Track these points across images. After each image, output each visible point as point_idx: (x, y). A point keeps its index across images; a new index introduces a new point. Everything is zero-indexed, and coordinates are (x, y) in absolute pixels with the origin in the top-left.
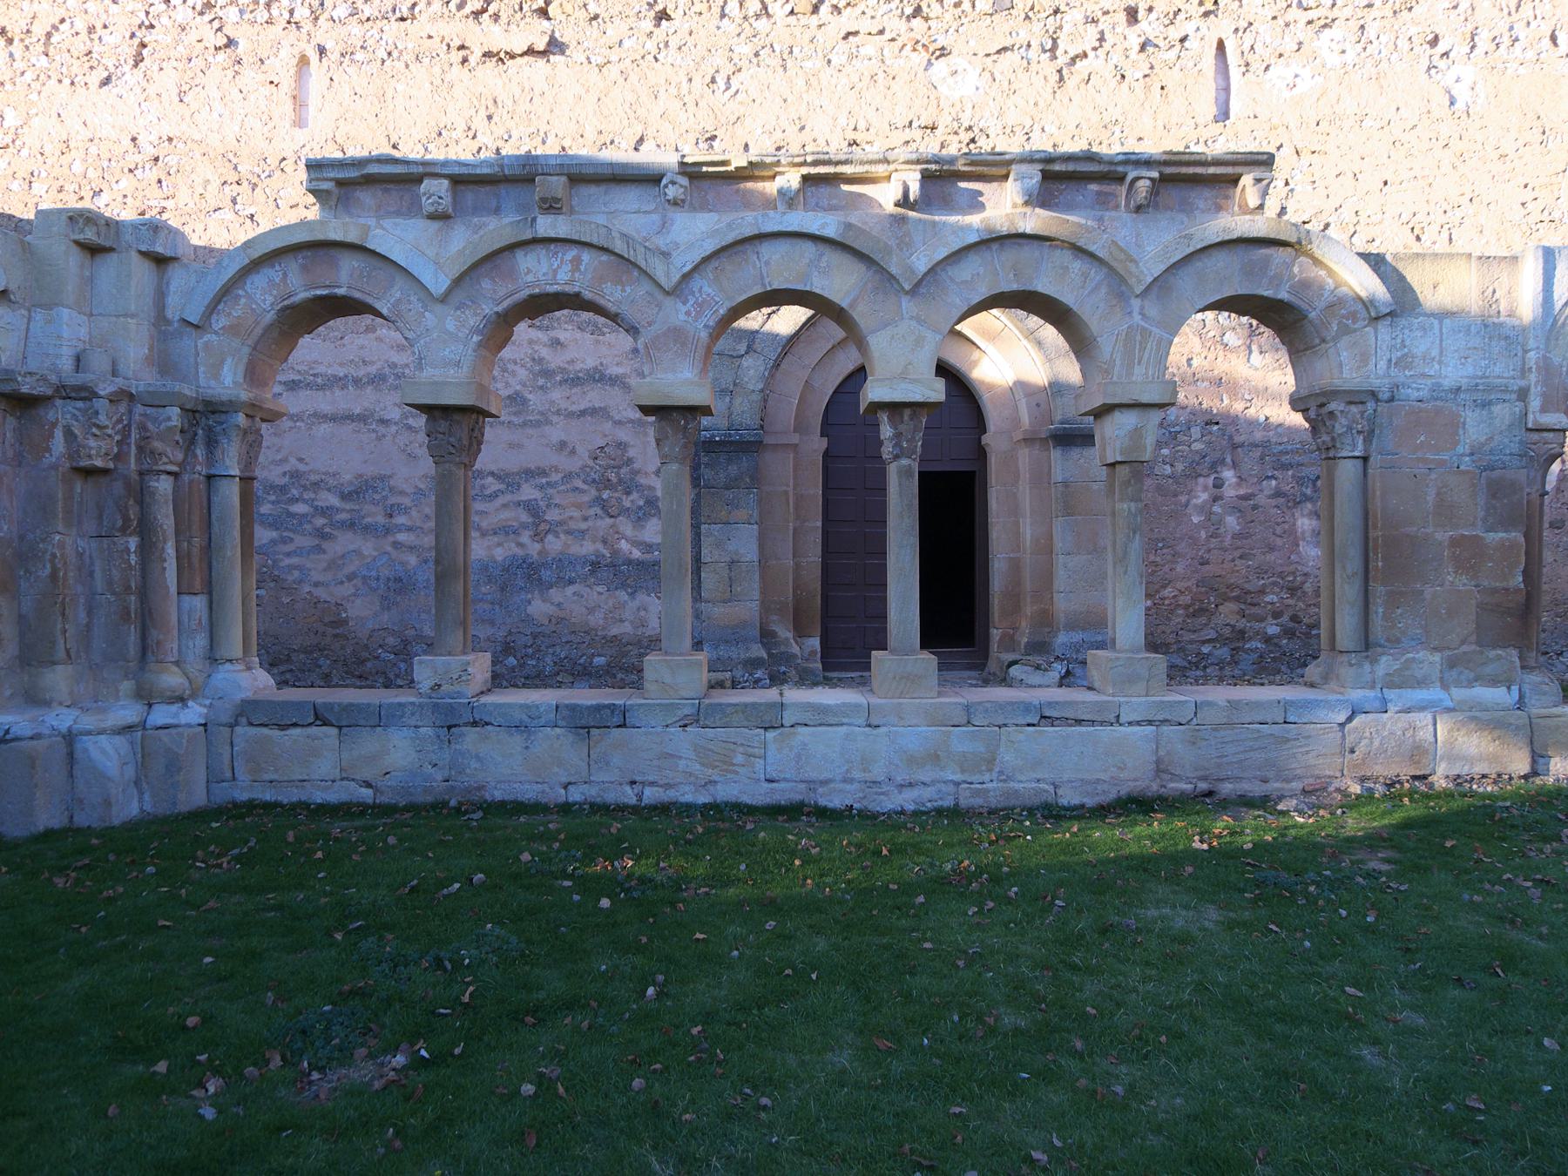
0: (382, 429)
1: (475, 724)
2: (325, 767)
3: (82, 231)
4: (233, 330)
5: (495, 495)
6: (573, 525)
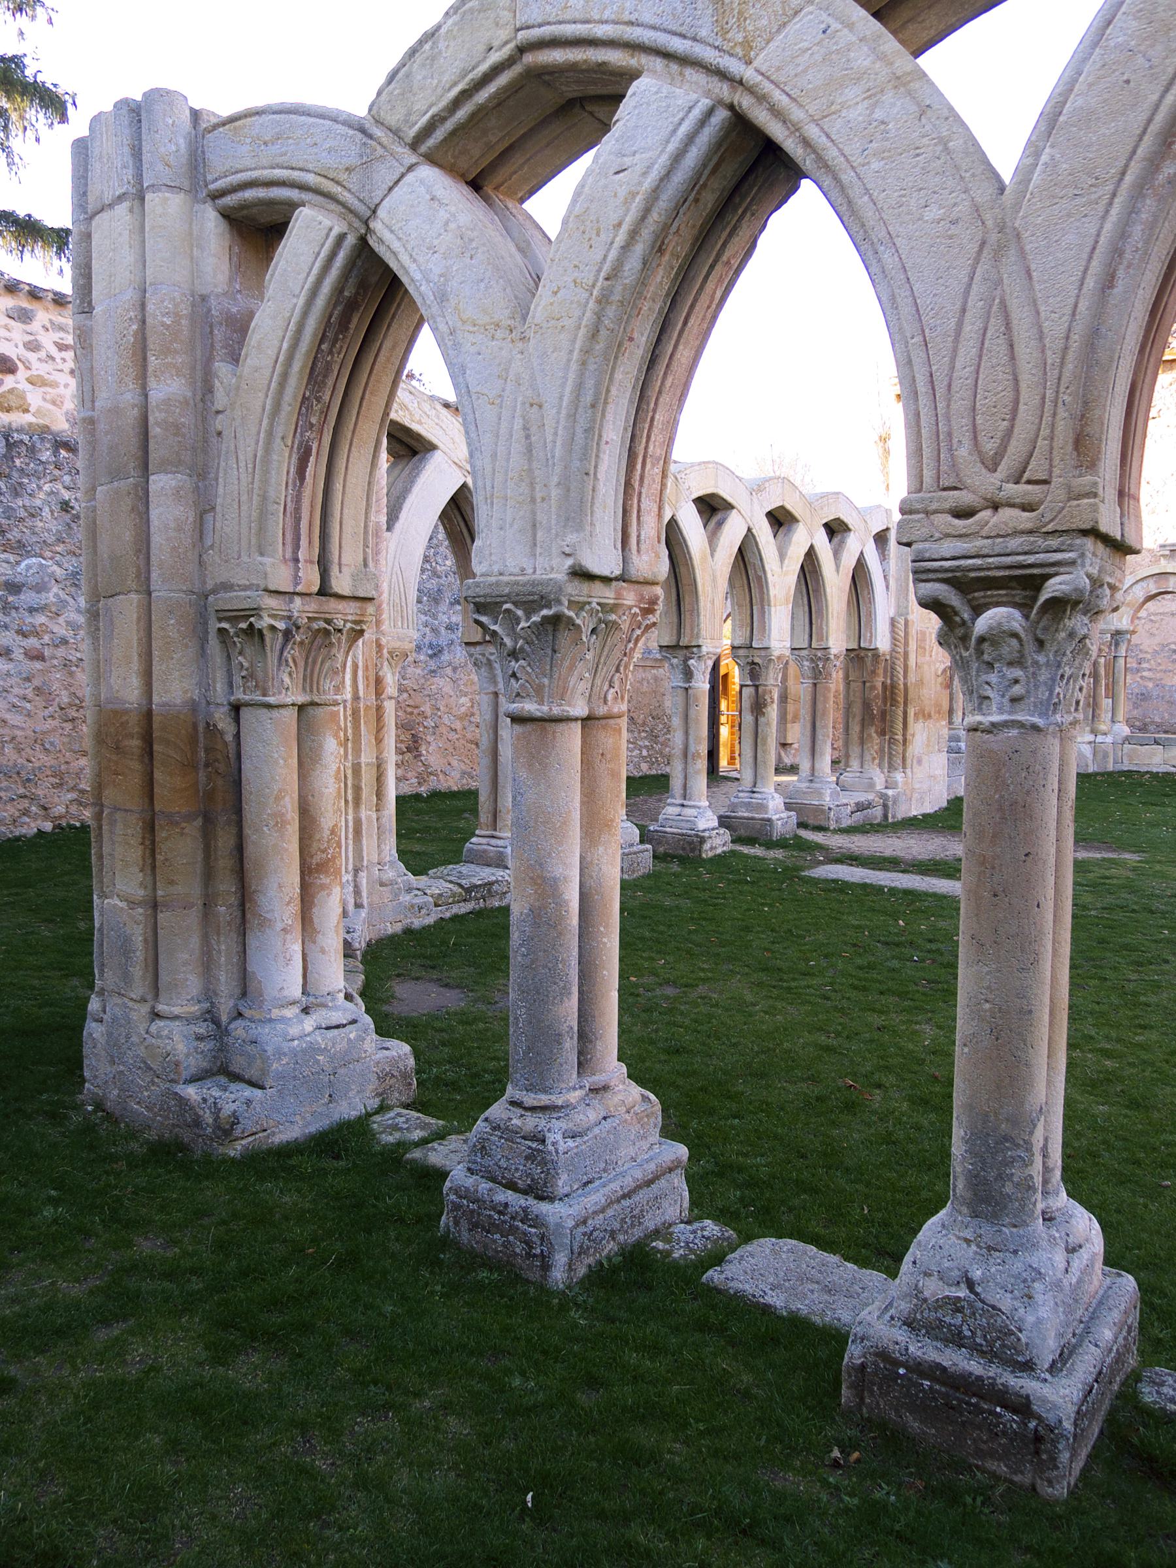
2: (1157, 759)
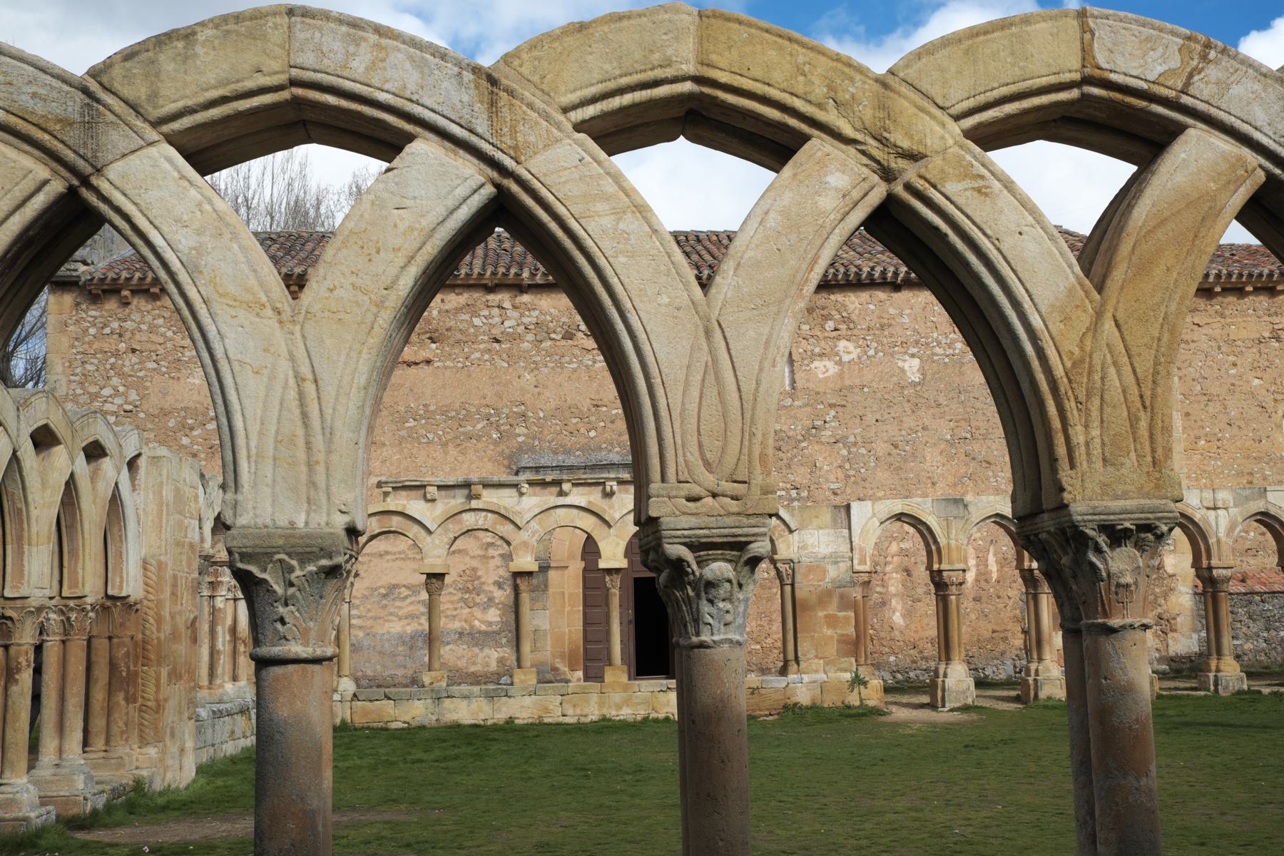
5: (406, 597)
6: (449, 613)
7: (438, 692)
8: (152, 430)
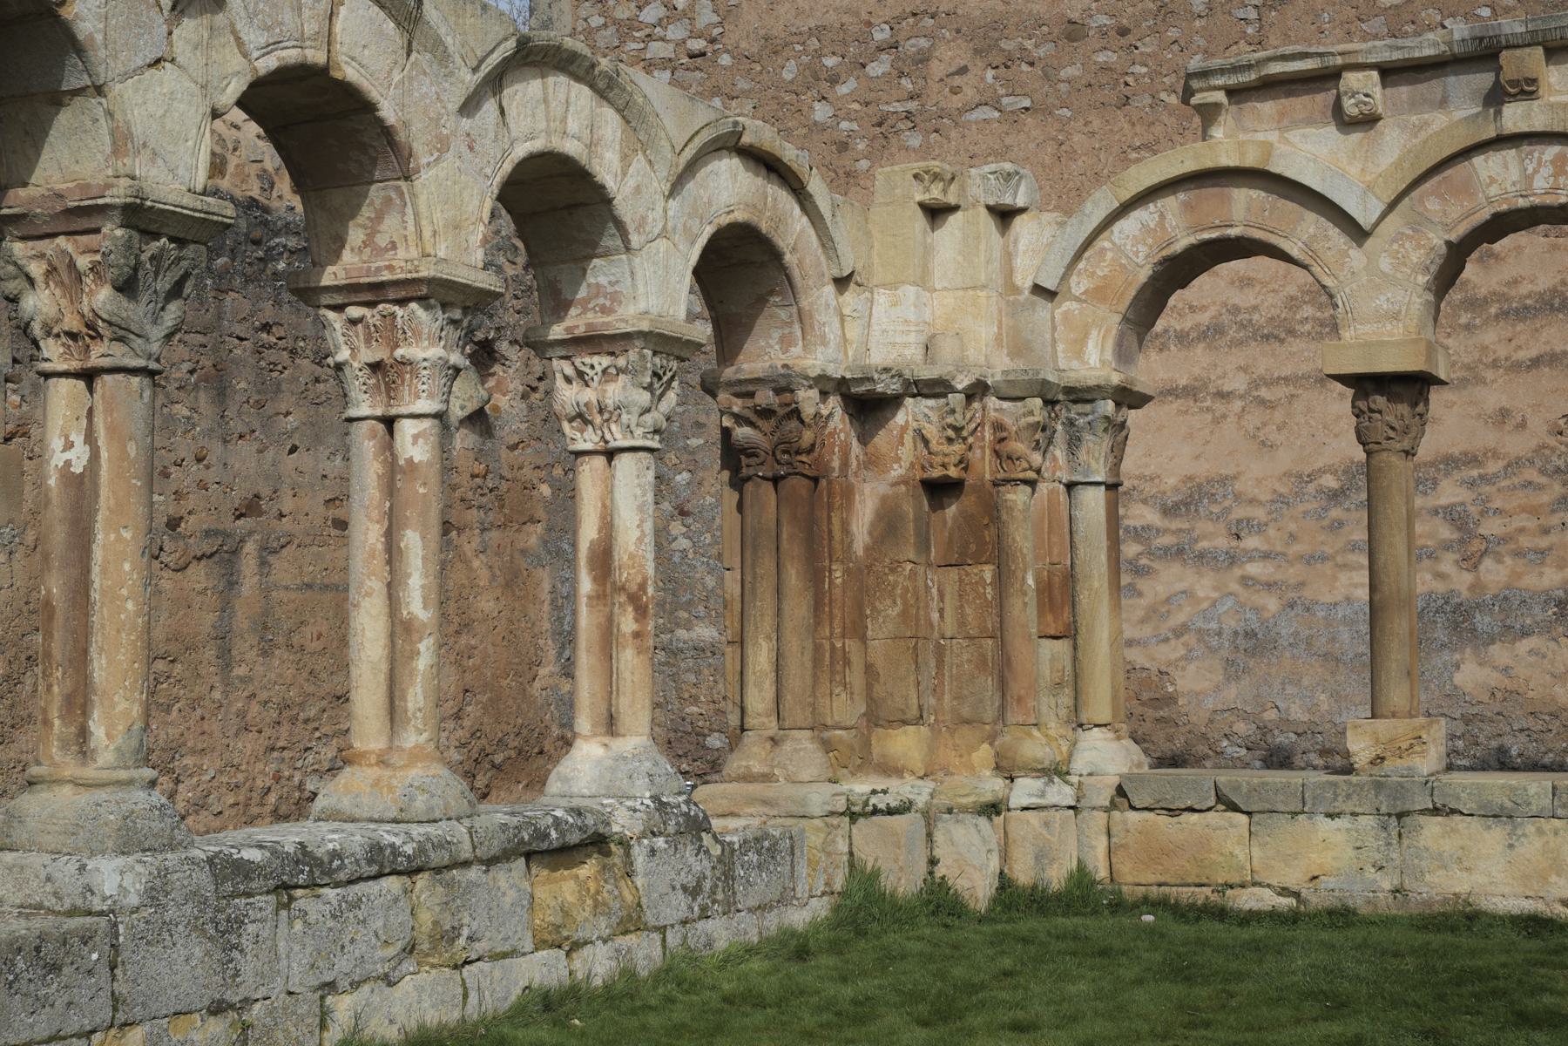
0: (1220, 407)
1: (1436, 811)
3: (927, 190)
4: (1098, 294)
6: (1525, 542)
7: (1400, 791)
8: (746, 94)
